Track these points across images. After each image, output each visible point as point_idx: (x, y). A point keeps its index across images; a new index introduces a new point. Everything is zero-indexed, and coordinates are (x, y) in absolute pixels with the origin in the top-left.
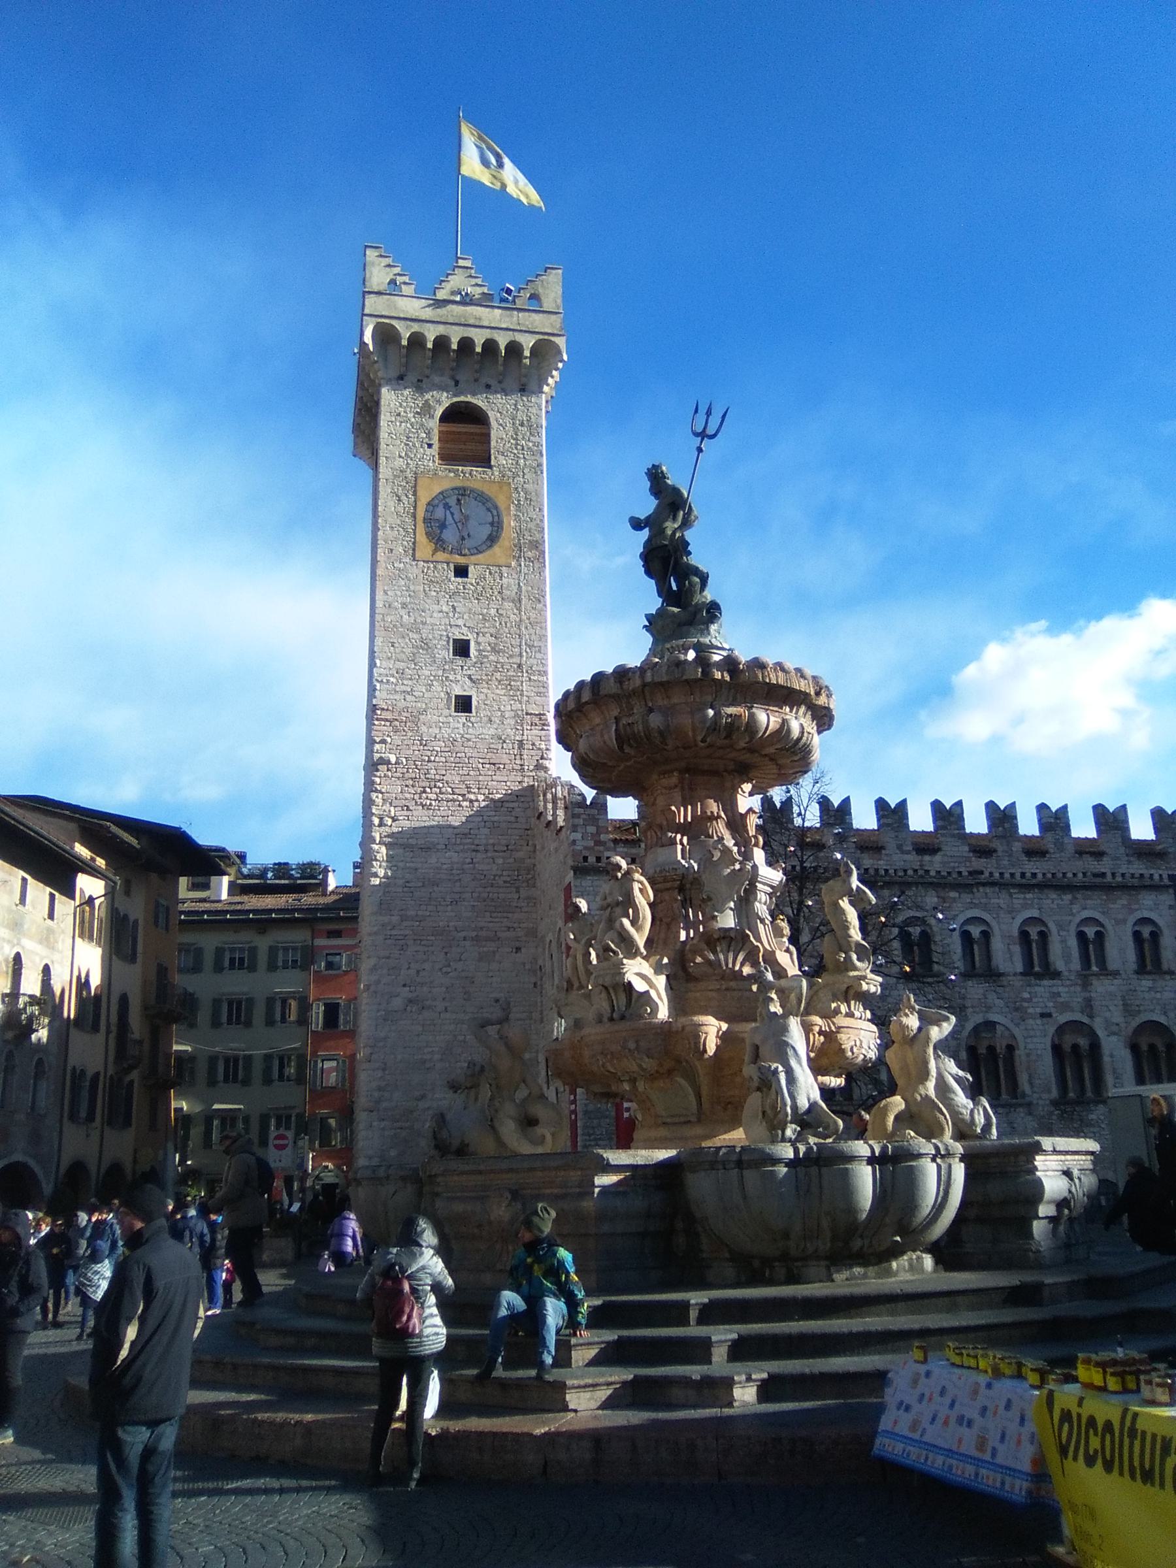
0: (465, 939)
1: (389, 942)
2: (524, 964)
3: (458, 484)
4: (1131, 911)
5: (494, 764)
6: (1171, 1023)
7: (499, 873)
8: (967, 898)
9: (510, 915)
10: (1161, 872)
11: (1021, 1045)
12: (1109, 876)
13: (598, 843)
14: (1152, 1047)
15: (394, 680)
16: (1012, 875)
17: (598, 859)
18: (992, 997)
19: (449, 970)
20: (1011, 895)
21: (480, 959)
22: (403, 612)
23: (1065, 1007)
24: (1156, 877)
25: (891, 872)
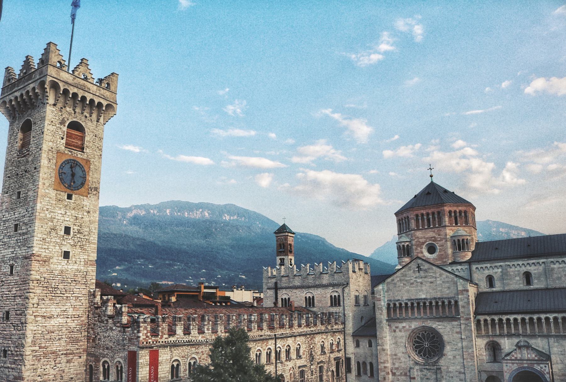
0: (62, 354)
1: (34, 358)
2: (82, 362)
3: (72, 158)
4: (267, 346)
5: (76, 281)
7: (75, 326)
9: (78, 343)
13: (147, 337)
15: (41, 243)
17: (147, 343)
19: (55, 368)
21: (67, 362)
22: (47, 212)
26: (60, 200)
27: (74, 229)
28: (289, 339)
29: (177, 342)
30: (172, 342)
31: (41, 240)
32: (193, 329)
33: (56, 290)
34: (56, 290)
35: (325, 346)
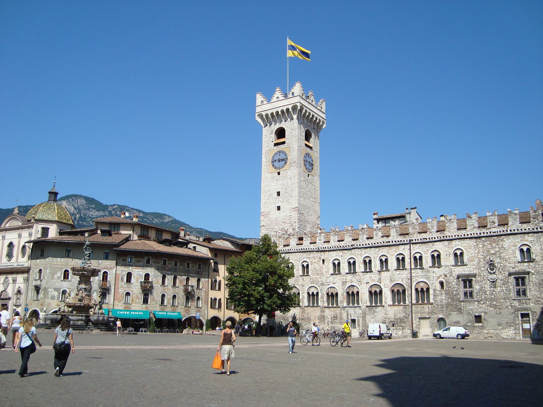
4: (396, 252)
6: (404, 283)
8: (350, 252)
10: (407, 239)
11: (360, 292)
12: (391, 242)
14: (398, 290)
15: (265, 205)
16: (363, 245)
18: (354, 279)
20: (361, 250)
22: (267, 187)
23: (374, 280)
24: (405, 241)
25: (332, 247)
26: (273, 178)
27: (282, 192)
28: (438, 243)
29: (291, 250)
30: (287, 250)
31: (264, 204)
32: (305, 241)
33: (273, 229)
34: (273, 229)
35: (532, 250)
